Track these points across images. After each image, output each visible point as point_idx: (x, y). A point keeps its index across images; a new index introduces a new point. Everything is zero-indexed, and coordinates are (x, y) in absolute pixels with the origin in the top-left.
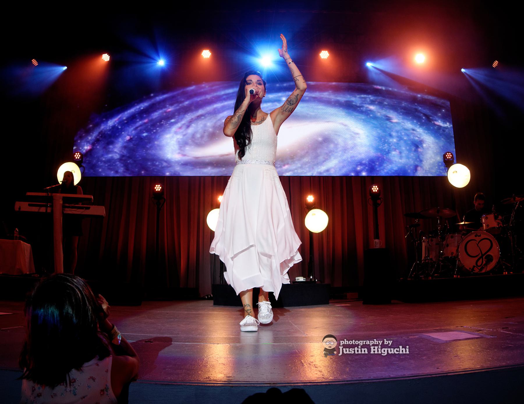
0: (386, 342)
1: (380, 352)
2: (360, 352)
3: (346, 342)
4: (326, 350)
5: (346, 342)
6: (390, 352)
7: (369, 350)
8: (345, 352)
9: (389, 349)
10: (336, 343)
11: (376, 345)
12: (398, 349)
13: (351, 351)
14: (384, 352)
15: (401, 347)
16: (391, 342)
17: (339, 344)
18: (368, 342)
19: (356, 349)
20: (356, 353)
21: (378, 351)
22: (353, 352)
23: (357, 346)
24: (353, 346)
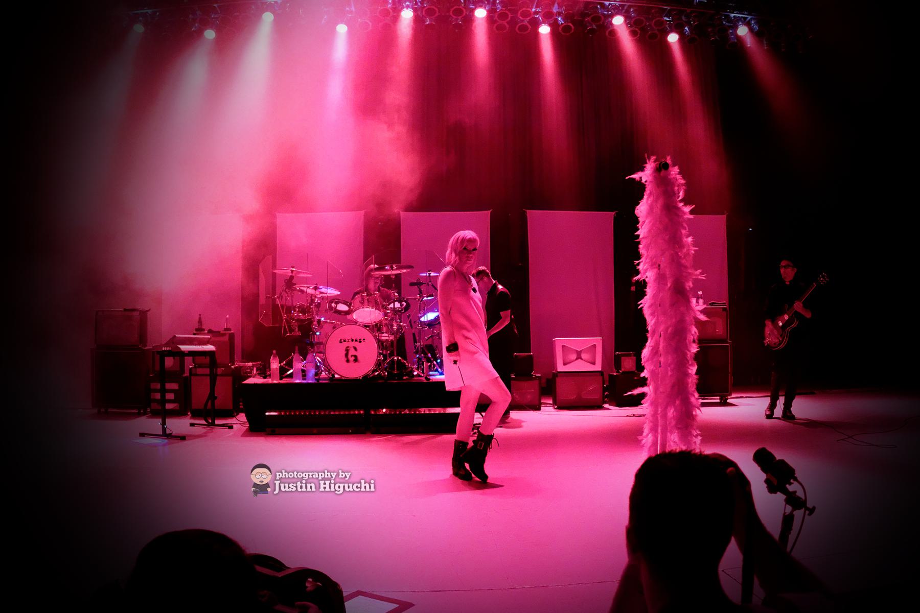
2: (304, 489)
4: (255, 485)
5: (284, 475)
6: (347, 489)
9: (346, 485)
11: (330, 479)
15: (363, 482)
20: (299, 489)
24: (294, 481)
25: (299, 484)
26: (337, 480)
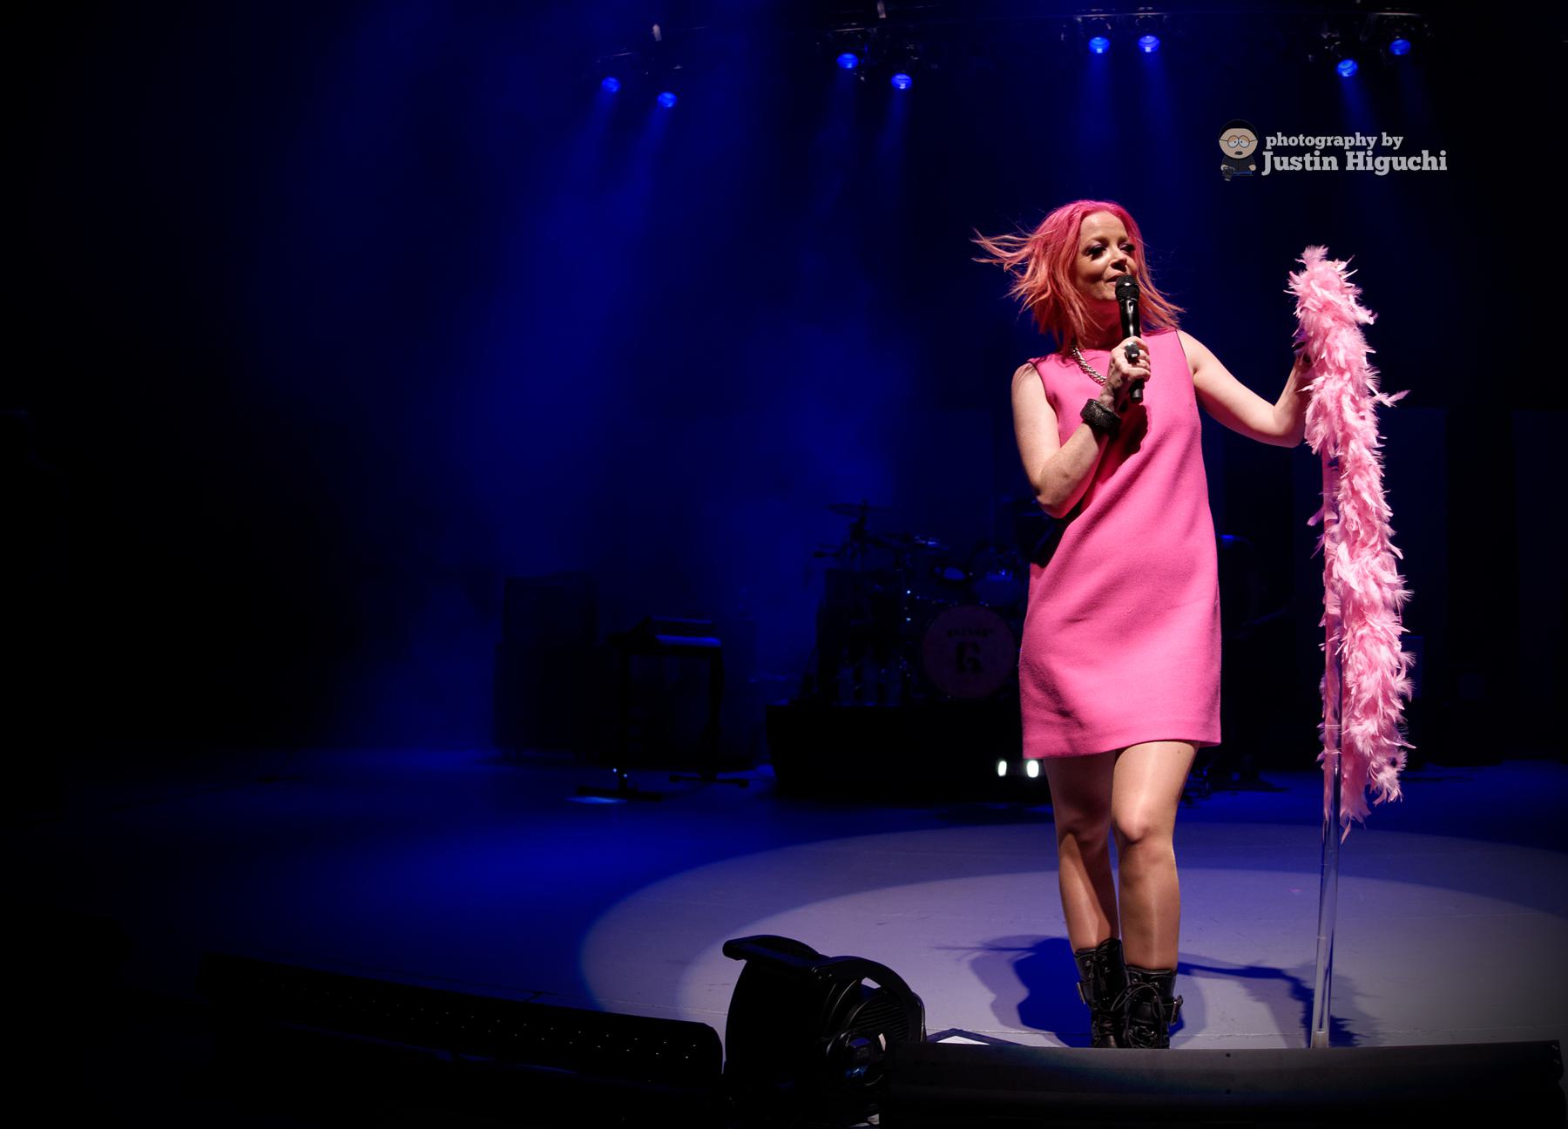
0: (1387, 140)
1: (1370, 167)
2: (1317, 167)
3: (1280, 140)
6: (1396, 167)
7: (1342, 162)
8: (1278, 167)
9: (1395, 159)
10: (1254, 144)
11: (1363, 149)
12: (1418, 160)
13: (1294, 164)
14: (1382, 166)
16: (1398, 141)
17: (1262, 146)
18: (1339, 141)
19: (1308, 158)
20: (1308, 168)
21: (1365, 164)
22: (1300, 167)
23: (1311, 150)
24: (1300, 151)
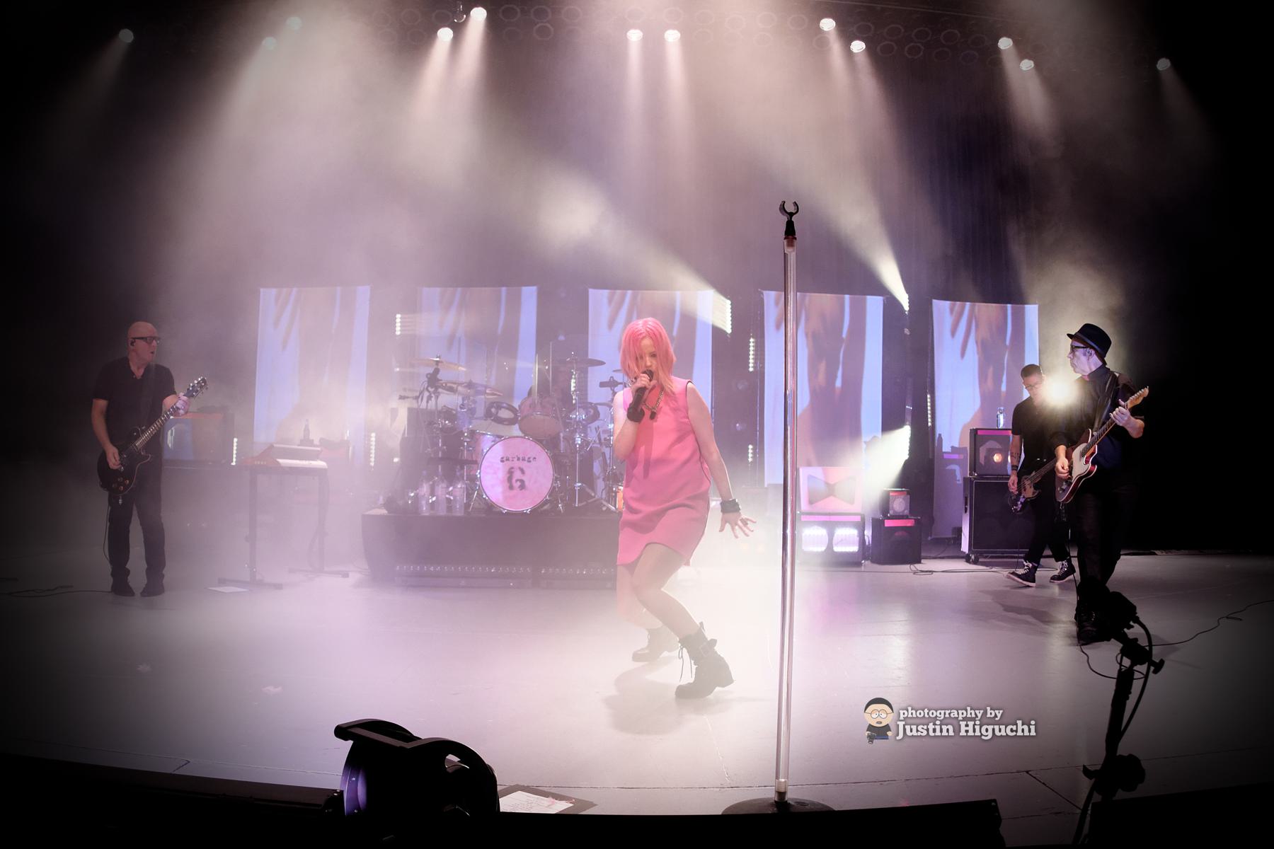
1: (978, 733)
2: (938, 733)
4: (871, 728)
6: (997, 733)
7: (957, 730)
9: (997, 728)
11: (973, 719)
14: (987, 732)
15: (1019, 722)
18: (954, 714)
20: (931, 733)
25: (931, 726)
26: (985, 721)
